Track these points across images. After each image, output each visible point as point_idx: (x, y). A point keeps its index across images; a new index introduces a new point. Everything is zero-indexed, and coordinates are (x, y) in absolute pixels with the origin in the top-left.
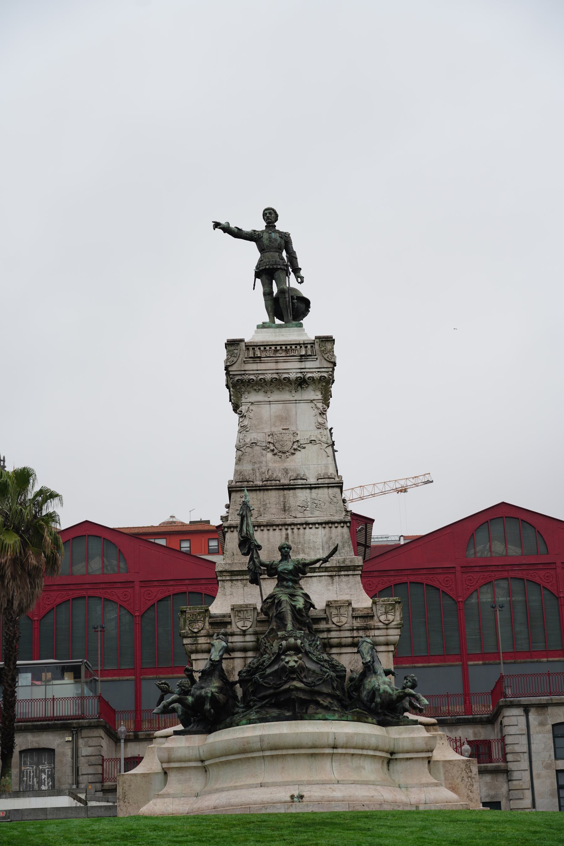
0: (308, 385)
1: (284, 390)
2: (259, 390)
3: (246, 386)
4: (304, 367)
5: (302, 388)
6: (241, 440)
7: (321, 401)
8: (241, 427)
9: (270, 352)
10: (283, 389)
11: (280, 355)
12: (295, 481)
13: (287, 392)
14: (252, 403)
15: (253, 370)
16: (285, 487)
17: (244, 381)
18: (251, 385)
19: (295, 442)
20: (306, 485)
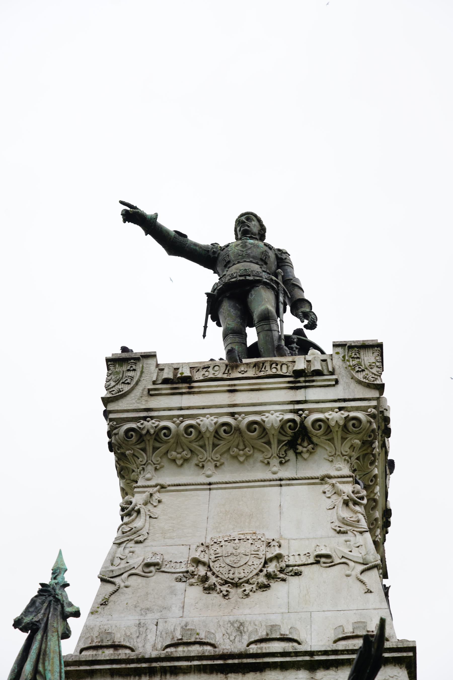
0: (316, 445)
1: (251, 461)
2: (186, 460)
3: (149, 449)
4: (303, 399)
5: (298, 454)
6: (117, 561)
7: (351, 479)
8: (123, 533)
9: (216, 368)
10: (248, 457)
11: (240, 375)
12: (264, 645)
13: (259, 465)
14: (163, 487)
15: (170, 409)
16: (230, 661)
17: (144, 432)
18: (164, 448)
19: (271, 560)
20: (297, 654)
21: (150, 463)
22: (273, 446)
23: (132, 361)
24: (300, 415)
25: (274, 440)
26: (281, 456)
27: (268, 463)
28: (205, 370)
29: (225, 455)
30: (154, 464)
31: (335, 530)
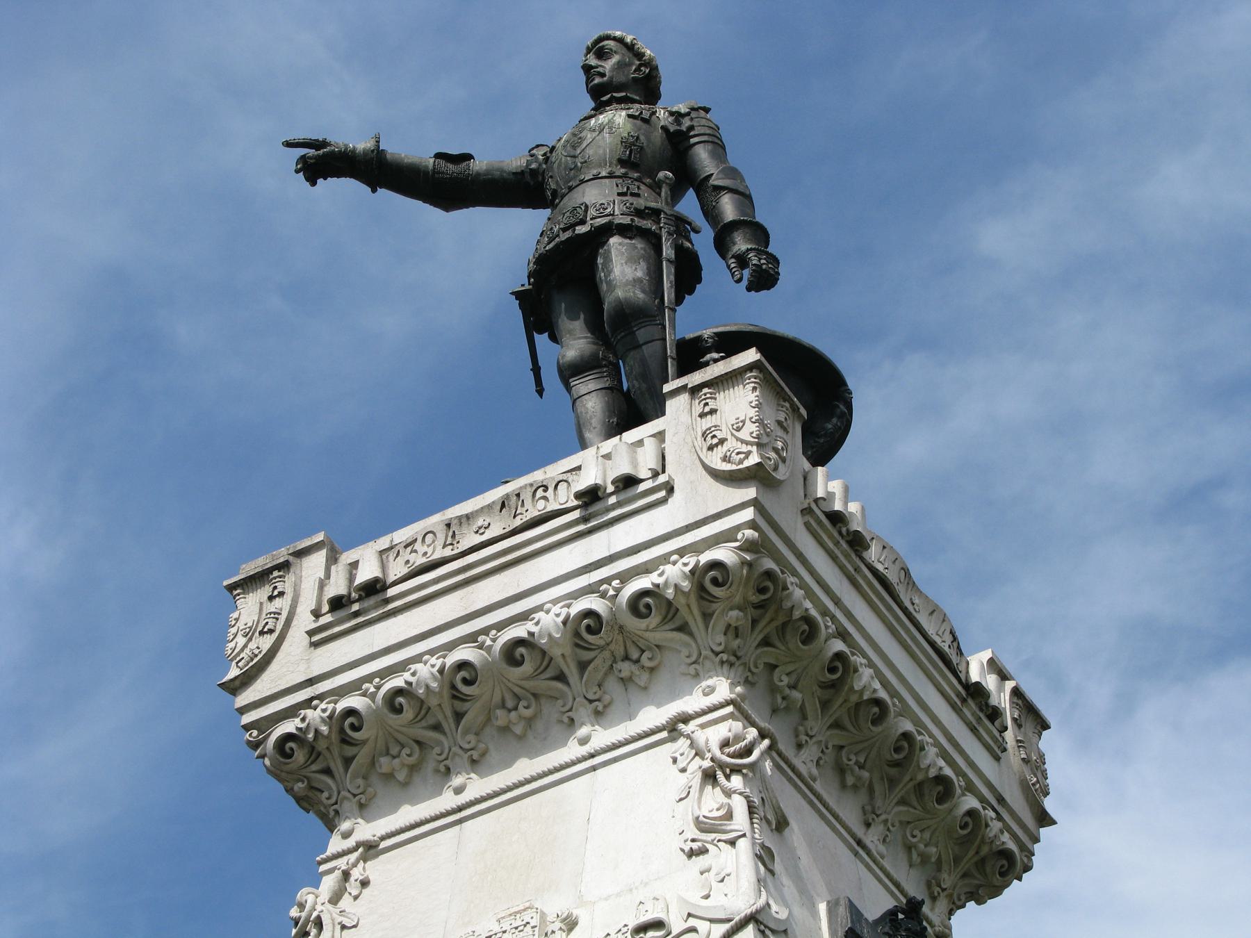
1: (539, 725)
7: (730, 709)
9: (429, 538)
10: (530, 721)
11: (478, 539)
17: (311, 736)
21: (345, 798)
22: (571, 681)
23: (276, 573)
24: (603, 595)
25: (568, 667)
26: (591, 697)
27: (572, 720)
28: (409, 549)
29: (488, 731)
30: (355, 796)
31: (682, 850)
